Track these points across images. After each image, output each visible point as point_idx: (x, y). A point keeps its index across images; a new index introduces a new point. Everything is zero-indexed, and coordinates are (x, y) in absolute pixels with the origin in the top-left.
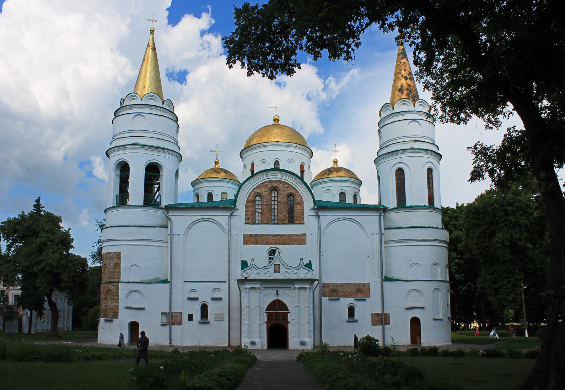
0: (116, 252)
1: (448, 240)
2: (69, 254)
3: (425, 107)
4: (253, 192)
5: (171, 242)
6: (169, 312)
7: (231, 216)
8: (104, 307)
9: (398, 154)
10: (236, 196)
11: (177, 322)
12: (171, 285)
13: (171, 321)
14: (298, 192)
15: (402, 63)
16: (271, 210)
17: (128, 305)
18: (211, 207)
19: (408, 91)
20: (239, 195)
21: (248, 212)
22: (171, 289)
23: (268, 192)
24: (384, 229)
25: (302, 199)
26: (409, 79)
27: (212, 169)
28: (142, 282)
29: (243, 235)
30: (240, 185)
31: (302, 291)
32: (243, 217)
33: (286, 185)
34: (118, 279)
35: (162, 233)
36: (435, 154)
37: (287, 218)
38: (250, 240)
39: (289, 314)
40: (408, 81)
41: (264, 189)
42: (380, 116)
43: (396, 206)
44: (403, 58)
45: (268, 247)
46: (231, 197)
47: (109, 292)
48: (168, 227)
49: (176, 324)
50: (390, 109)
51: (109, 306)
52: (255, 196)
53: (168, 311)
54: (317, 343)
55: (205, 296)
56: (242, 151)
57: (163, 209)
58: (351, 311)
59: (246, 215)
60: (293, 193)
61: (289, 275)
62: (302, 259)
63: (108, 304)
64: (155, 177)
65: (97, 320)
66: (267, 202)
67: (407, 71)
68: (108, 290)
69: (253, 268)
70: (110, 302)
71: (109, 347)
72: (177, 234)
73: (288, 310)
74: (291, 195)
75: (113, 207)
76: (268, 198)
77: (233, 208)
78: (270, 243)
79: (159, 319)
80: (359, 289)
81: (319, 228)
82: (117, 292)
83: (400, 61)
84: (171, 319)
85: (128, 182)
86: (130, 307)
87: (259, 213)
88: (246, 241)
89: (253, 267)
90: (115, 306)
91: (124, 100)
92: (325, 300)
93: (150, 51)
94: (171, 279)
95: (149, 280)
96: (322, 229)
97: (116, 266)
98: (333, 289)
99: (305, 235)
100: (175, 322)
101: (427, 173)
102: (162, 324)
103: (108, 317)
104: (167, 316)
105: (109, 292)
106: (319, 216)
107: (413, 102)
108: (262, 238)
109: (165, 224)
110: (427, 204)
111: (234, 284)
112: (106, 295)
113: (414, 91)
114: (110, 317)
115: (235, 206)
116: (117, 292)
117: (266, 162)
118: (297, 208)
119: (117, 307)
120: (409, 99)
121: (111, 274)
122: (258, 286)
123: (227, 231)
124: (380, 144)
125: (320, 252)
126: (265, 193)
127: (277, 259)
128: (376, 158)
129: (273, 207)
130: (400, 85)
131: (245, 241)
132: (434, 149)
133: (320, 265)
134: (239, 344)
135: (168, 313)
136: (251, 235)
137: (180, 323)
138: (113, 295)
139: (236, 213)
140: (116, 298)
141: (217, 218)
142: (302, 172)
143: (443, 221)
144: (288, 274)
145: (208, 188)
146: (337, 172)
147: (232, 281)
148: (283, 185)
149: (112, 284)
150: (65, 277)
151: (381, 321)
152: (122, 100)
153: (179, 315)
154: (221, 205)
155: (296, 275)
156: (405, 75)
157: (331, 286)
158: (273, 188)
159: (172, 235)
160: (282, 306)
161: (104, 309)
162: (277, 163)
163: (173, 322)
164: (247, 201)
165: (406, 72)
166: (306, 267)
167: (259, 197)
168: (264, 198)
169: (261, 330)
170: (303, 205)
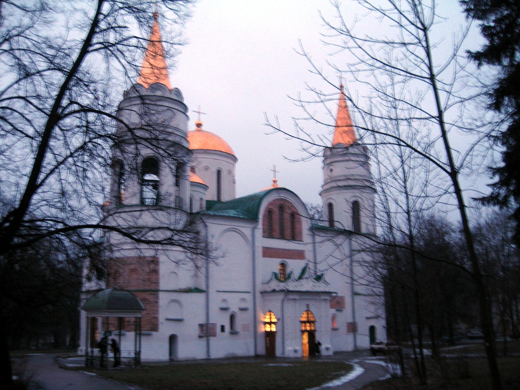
38: (268, 253)
45: (279, 261)
55: (234, 308)
79: (195, 331)
111: (258, 295)
119: (156, 319)
122: (296, 297)
136: (267, 248)
137: (214, 335)
149: (149, 293)
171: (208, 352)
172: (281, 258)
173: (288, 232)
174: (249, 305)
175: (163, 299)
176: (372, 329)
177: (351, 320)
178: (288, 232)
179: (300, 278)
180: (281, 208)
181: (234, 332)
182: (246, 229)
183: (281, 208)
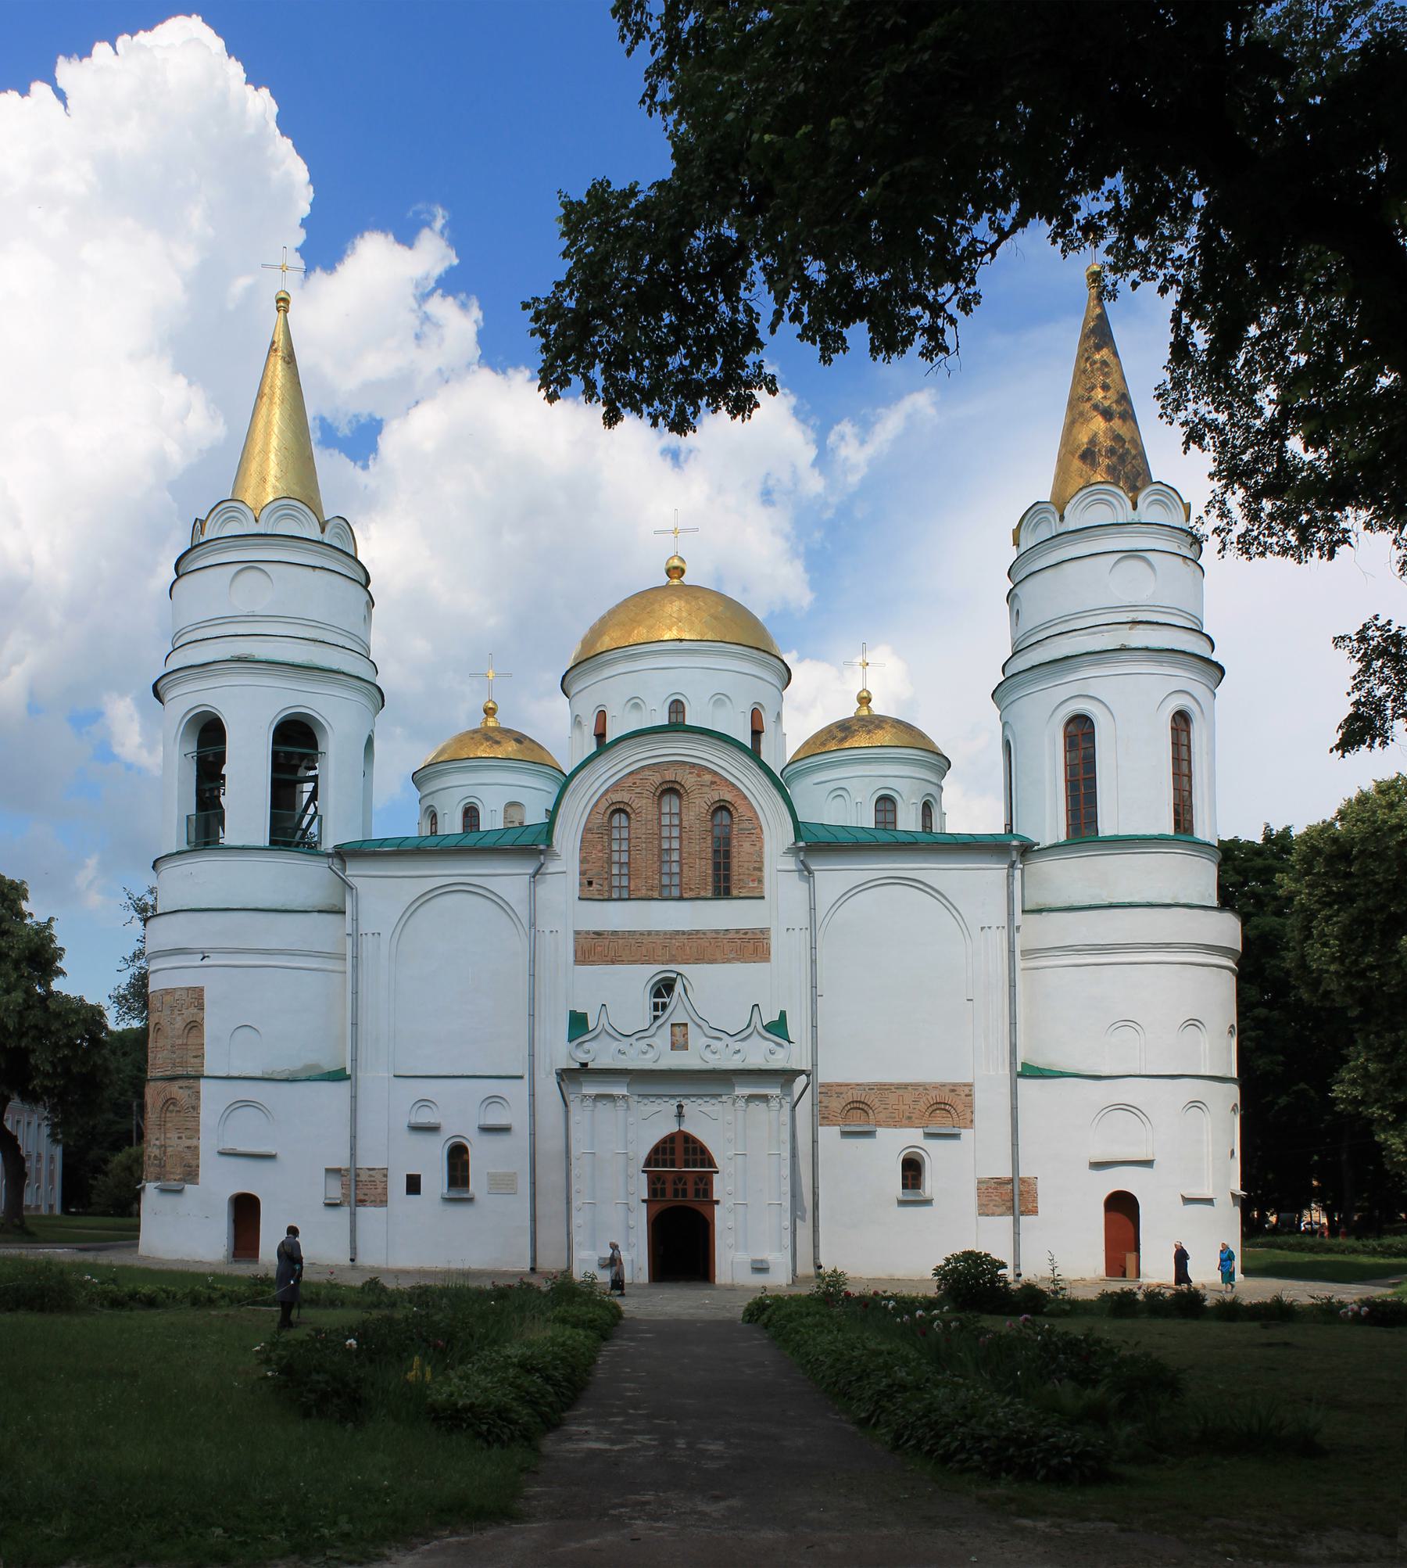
0: (188, 989)
1: (1239, 947)
2: (50, 994)
3: (1170, 510)
4: (603, 800)
5: (356, 957)
6: (348, 1166)
7: (537, 877)
8: (156, 1152)
9: (1075, 669)
10: (553, 814)
11: (373, 1198)
12: (356, 1087)
13: (356, 1197)
14: (746, 798)
15: (1095, 362)
16: (659, 856)
17: (229, 1146)
18: (476, 849)
19: (1114, 459)
20: (561, 811)
21: (588, 862)
22: (354, 1098)
23: (651, 801)
24: (1024, 911)
25: (757, 818)
26: (1119, 418)
27: (475, 731)
28: (267, 1076)
29: (571, 936)
30: (563, 779)
31: (757, 1108)
32: (574, 879)
33: (708, 778)
34: (195, 1069)
35: (322, 931)
36: (1200, 664)
37: (710, 879)
40: (1116, 423)
41: (638, 790)
42: (1016, 543)
43: (1063, 838)
44: (1098, 348)
45: (646, 974)
46: (534, 816)
47: (171, 1108)
48: (345, 913)
49: (372, 1202)
50: (1051, 519)
51: (171, 1149)
52: (609, 812)
53: (344, 1164)
54: (806, 1268)
56: (567, 672)
57: (328, 855)
58: (912, 1170)
59: (582, 873)
60: (730, 803)
61: (717, 1056)
62: (756, 1008)
63: (167, 1140)
64: (302, 760)
65: (138, 1187)
66: (648, 832)
67: (1112, 390)
68: (167, 1101)
69: (604, 1035)
70: (173, 1135)
71: (175, 1268)
72: (373, 934)
74: (722, 808)
75: (179, 853)
76: (650, 817)
77: (541, 852)
78: (656, 958)
79: (320, 1188)
80: (937, 1103)
81: (812, 909)
83: (1087, 359)
84: (356, 1189)
85: (223, 777)
86: (231, 1152)
87: (621, 864)
88: (583, 953)
89: (604, 1033)
90: (188, 1147)
91: (203, 523)
92: (829, 1134)
93: (279, 367)
94: (354, 1067)
95: (287, 1072)
96: (821, 912)
97: (191, 1029)
98: (853, 1102)
99: (764, 931)
100: (366, 1198)
101: (1172, 728)
102: (328, 1201)
103: (168, 1180)
104: (344, 1178)
105: (171, 1108)
106: (810, 872)
107: (1130, 495)
108: (633, 941)
109: (335, 901)
110: (1169, 830)
111: (548, 1085)
112: (163, 1115)
113: (1134, 457)
115: (549, 845)
116: (193, 1108)
117: (642, 705)
118: (741, 850)
119: (194, 1150)
120: (1116, 484)
121: (174, 1052)
123: (525, 921)
124: (1012, 638)
125: (814, 987)
126: (643, 804)
127: (680, 1006)
128: (1000, 684)
129: (666, 846)
130: (1085, 440)
131: (579, 954)
132: (1201, 648)
133: (814, 1027)
134: (564, 1267)
135: (346, 1170)
137: (383, 1203)
138: (181, 1114)
139: (552, 867)
140: (190, 1125)
141: (493, 884)
142: (756, 734)
143: (1221, 888)
144: (715, 1053)
145: (466, 792)
146: (869, 732)
147: (540, 1075)
148: (699, 776)
149: (181, 1083)
150: (40, 1059)
151: (1009, 1204)
152: (198, 524)
153: (378, 1177)
154: (507, 840)
156: (1107, 403)
157: (850, 1094)
158: (665, 786)
159: (356, 936)
160: (695, 1149)
161: (155, 1156)
162: (677, 707)
163: (362, 1197)
164: (587, 830)
165: (1109, 394)
166: (767, 1031)
167: (623, 815)
168: (639, 819)
169: (631, 1223)
170: (760, 839)
171: (354, 1248)
172: (655, 962)
174: (515, 1115)
175: (212, 1098)
181: (465, 1196)
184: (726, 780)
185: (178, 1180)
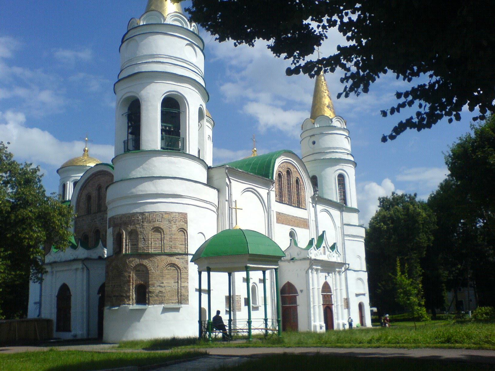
25: (304, 185)
39: (332, 296)
73: (330, 292)
82: (185, 268)
90: (183, 287)
97: (181, 231)
114: (173, 303)
119: (186, 288)
136: (279, 213)
141: (259, 190)
149: (177, 257)
155: (333, 258)
173: (294, 198)
176: (361, 306)
177: (345, 296)
178: (294, 198)
179: (318, 246)
180: (289, 173)
182: (263, 192)
183: (289, 173)
184: (298, 172)
185: (175, 303)
